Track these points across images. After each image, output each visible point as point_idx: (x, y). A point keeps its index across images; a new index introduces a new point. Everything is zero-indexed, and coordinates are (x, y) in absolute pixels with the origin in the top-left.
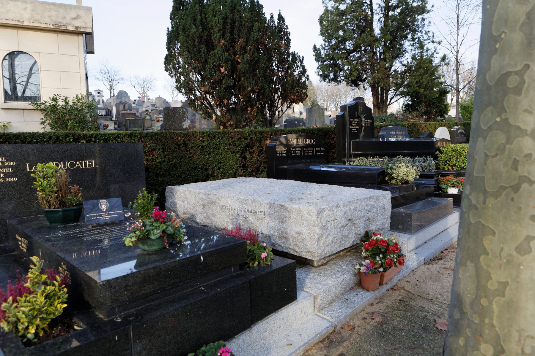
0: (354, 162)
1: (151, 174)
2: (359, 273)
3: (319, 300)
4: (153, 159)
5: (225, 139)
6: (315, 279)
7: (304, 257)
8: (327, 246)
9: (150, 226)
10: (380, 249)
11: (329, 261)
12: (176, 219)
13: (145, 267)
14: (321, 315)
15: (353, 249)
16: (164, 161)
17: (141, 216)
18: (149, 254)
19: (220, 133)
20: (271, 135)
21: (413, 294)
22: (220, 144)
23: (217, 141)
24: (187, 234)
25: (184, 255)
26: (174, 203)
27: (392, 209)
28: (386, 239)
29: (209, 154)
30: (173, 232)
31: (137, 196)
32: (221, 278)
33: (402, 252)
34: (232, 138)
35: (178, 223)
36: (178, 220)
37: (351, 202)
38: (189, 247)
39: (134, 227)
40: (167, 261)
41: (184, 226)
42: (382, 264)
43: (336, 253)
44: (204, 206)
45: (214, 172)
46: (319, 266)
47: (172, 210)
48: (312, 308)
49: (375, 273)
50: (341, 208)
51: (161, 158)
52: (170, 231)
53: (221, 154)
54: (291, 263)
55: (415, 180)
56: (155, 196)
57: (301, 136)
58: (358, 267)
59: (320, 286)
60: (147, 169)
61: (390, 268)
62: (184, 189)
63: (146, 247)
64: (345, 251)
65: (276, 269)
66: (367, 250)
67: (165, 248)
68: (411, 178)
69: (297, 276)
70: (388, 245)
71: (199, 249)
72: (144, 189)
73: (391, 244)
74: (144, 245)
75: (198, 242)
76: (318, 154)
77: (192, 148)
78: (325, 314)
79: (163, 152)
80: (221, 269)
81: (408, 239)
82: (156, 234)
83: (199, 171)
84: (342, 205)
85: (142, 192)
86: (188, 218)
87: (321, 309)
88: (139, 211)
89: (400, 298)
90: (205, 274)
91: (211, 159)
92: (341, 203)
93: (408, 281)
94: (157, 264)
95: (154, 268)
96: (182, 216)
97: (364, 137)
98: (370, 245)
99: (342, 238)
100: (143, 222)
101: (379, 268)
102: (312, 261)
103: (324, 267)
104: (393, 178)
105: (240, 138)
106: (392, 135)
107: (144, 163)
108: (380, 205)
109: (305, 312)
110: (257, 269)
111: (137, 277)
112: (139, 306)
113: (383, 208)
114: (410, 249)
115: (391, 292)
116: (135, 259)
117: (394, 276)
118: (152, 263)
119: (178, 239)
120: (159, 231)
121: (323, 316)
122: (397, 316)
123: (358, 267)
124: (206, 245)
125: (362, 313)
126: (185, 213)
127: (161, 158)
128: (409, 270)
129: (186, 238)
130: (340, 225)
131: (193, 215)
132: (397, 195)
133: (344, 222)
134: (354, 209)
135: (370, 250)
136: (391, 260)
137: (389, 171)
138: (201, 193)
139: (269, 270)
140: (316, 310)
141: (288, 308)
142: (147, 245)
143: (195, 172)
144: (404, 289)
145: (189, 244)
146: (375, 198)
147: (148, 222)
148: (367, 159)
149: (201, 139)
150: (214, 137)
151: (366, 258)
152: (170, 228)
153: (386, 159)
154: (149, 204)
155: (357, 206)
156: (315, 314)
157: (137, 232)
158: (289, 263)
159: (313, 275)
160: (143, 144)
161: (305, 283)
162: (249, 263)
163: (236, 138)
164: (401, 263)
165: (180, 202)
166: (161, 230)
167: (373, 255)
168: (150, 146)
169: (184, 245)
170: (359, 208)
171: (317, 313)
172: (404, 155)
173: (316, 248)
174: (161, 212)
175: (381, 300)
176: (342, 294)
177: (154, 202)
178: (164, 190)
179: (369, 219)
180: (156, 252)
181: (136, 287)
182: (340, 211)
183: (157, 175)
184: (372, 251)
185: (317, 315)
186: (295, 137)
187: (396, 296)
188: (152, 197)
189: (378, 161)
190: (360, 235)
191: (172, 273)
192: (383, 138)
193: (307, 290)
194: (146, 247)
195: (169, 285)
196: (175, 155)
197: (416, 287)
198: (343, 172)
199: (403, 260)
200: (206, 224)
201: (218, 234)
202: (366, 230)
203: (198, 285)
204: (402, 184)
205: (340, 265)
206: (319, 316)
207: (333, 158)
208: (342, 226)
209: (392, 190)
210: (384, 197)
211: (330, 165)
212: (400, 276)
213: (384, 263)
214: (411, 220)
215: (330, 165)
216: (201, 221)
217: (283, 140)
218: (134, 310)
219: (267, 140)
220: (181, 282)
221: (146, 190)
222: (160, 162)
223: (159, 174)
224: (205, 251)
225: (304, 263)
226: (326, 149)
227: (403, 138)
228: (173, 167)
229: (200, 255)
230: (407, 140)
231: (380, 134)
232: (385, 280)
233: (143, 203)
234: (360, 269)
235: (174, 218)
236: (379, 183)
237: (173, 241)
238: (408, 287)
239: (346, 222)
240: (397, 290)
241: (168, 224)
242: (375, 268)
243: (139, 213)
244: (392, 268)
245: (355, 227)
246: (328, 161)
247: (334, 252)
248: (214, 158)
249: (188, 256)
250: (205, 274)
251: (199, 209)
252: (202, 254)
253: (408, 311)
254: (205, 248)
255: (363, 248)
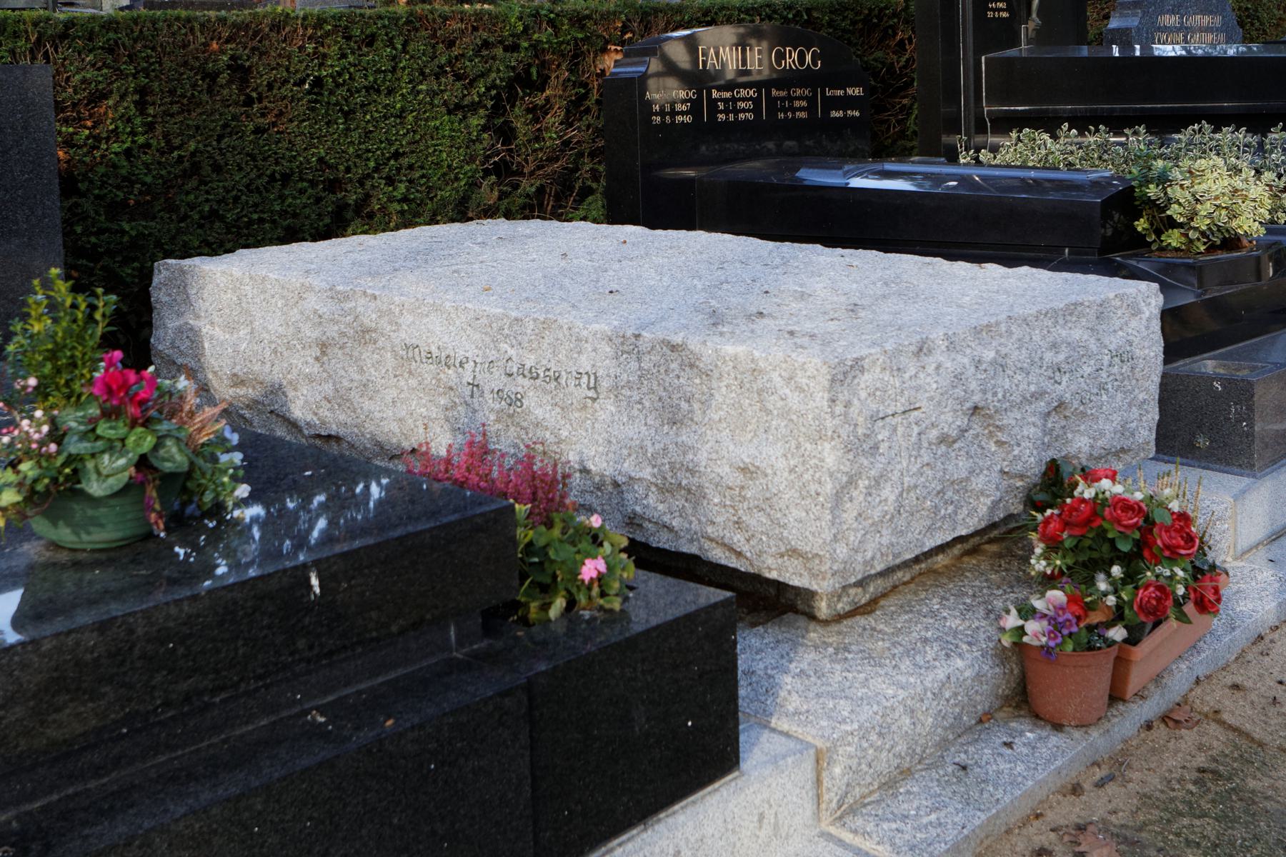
0: (995, 149)
1: (87, 205)
2: (1019, 647)
3: (837, 770)
4: (97, 139)
5: (417, 46)
6: (820, 674)
7: (773, 575)
8: (876, 527)
9: (84, 436)
10: (1112, 541)
11: (884, 596)
12: (199, 407)
13: (60, 624)
14: (847, 837)
15: (990, 541)
16: (147, 145)
17: (42, 392)
18: (76, 565)
19: (395, 19)
20: (625, 29)
21: (1261, 745)
22: (394, 70)
23: (380, 56)
24: (248, 473)
25: (235, 566)
26: (193, 336)
27: (1166, 361)
28: (1139, 496)
29: (346, 115)
30: (185, 467)
31: (25, 304)
32: (400, 671)
33: (1211, 556)
34: (451, 44)
35: (207, 424)
36: (209, 411)
37: (983, 332)
38: (256, 533)
39: (11, 445)
40: (160, 597)
41: (235, 438)
42: (1119, 607)
43: (917, 560)
44: (324, 346)
45: (368, 196)
46: (840, 618)
47: (181, 368)
48: (809, 808)
49: (1090, 648)
50: (939, 357)
51: (133, 133)
52: (170, 459)
53: (401, 115)
54: (715, 606)
55: (1269, 232)
56: (106, 302)
57: (758, 34)
58: (1012, 621)
59: (844, 707)
60: (69, 183)
61: (1157, 624)
62: (237, 272)
63: (64, 534)
64: (957, 550)
65: (647, 632)
66: (1053, 545)
67: (150, 536)
68: (1249, 224)
69: (742, 664)
70: (1150, 522)
71: (301, 542)
72: (55, 271)
73: (1161, 517)
74: (55, 525)
75: (295, 513)
76: (835, 114)
77: (270, 86)
78: (865, 834)
79: (141, 106)
80: (402, 632)
81: (1239, 496)
82: (108, 473)
83: (302, 191)
84: (943, 345)
85: (47, 284)
86: (254, 404)
87: (848, 810)
88: (34, 368)
89: (1201, 760)
90: (331, 653)
91: (355, 135)
92: (937, 335)
93: (1236, 687)
94: (116, 609)
95: (102, 627)
96: (224, 391)
97: (1041, 37)
98: (1066, 525)
99: (941, 492)
100: (53, 422)
101: (1110, 625)
102: (809, 595)
103: (861, 621)
104: (1172, 223)
105: (486, 44)
106: (1165, 29)
107: (54, 155)
108: (1114, 342)
109: (776, 826)
110: (560, 629)
111: (24, 666)
112: (31, 797)
113: (1123, 356)
114: (1244, 543)
115: (1161, 732)
116: (14, 586)
117: (1178, 662)
118: (92, 603)
119: (208, 497)
120: (122, 462)
121: (857, 841)
122: (1188, 843)
123: (1012, 621)
124: (332, 523)
125: (1031, 830)
126: (237, 381)
127: (133, 133)
128: (1240, 638)
129: (243, 490)
130: (934, 434)
131: (276, 391)
132: (1186, 298)
133: (950, 421)
134: (993, 362)
135: (1068, 544)
136: (1161, 588)
137: (1152, 191)
138: (310, 288)
139: (613, 635)
140: (825, 815)
141: (699, 808)
142: (68, 525)
143: (282, 198)
144: (1222, 723)
145: (255, 520)
146: (1091, 313)
147: (72, 419)
148: (1055, 137)
149: (310, 47)
150: (370, 40)
151: (1048, 581)
152: (171, 447)
153: (1138, 140)
154: (80, 339)
155: (1010, 347)
156: (822, 834)
157: (24, 467)
158: (702, 602)
159: (811, 656)
160: (51, 69)
161: (775, 695)
162: (526, 605)
163: (467, 43)
164: (1207, 605)
165: (218, 332)
166: (133, 456)
167: (1082, 570)
168: (84, 81)
169: (237, 522)
170: (1019, 357)
171: (832, 830)
172: (1218, 121)
173: (828, 536)
174: (132, 376)
175: (1115, 768)
176: (944, 744)
177: (99, 330)
178: (146, 276)
179: (1061, 406)
180: (108, 557)
181: (19, 711)
182: (931, 369)
183: (116, 209)
184: (1074, 549)
185: (829, 837)
186: (734, 39)
187: (1185, 751)
188: (93, 308)
189: (1104, 147)
190: (1022, 477)
191: (181, 651)
192: (1126, 45)
193: (784, 725)
194: (64, 534)
195: (167, 704)
196: (194, 118)
197: (1272, 711)
198: (948, 197)
199: (1216, 591)
200: (334, 429)
201: (387, 472)
202: (1051, 454)
203: (295, 702)
204: (1212, 248)
205: (933, 614)
206: (840, 843)
207: (902, 135)
208: (944, 439)
209: (1167, 275)
210: (1129, 311)
211: (889, 166)
212: (1201, 663)
213: (1131, 603)
214: (1250, 409)
215: (889, 166)
216: (309, 417)
217: (678, 53)
218: (11, 813)
219: (604, 50)
220: (222, 689)
221: (67, 277)
222: (128, 153)
223: (124, 203)
224: (326, 553)
225: (771, 602)
226: (870, 91)
227: (1213, 46)
228: (186, 175)
229: (305, 567)
230: (1231, 52)
231: (1114, 23)
232: (1135, 680)
233: (53, 337)
234: (1021, 631)
235: (192, 400)
236: (1109, 246)
237: (184, 505)
238: (1238, 712)
239: (962, 421)
240: (1189, 723)
241: (164, 427)
242: (1090, 628)
243: (32, 382)
244: (1163, 629)
245: (1000, 443)
246: (882, 148)
247: (908, 556)
248: (368, 133)
249: (252, 573)
250: (331, 653)
251: (303, 362)
252: (317, 564)
253: (1235, 820)
254: (327, 538)
255: (1034, 536)
